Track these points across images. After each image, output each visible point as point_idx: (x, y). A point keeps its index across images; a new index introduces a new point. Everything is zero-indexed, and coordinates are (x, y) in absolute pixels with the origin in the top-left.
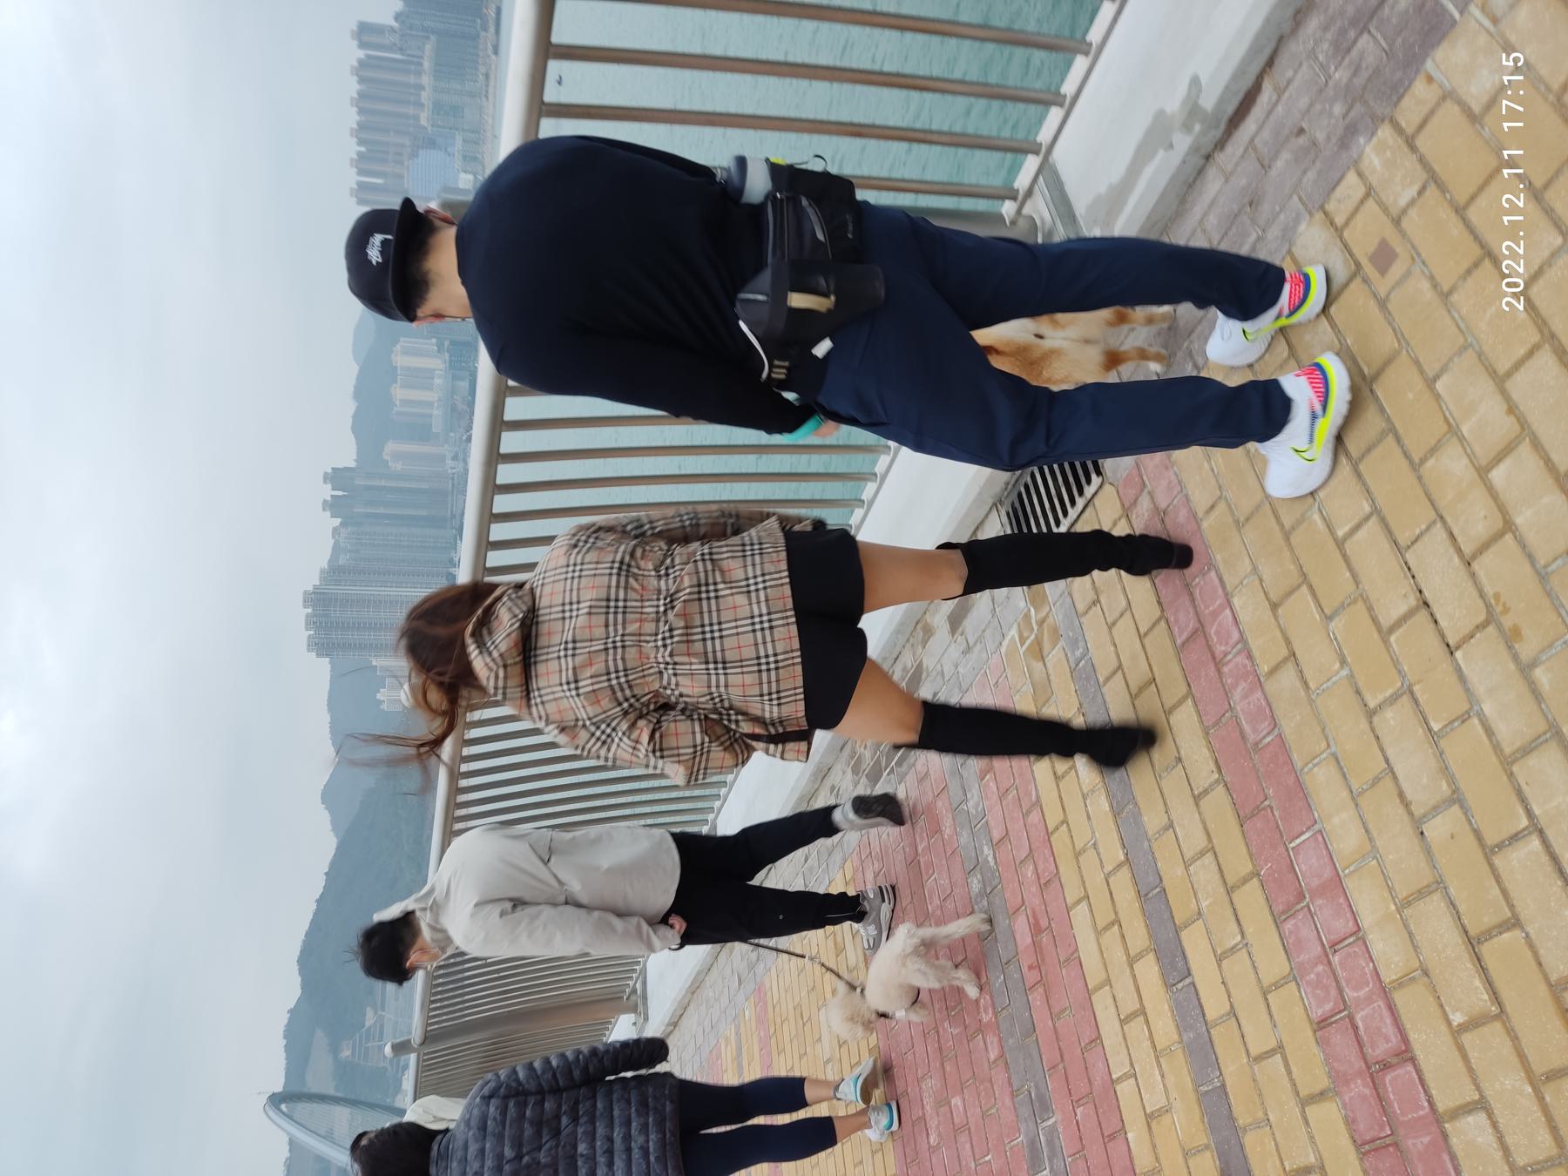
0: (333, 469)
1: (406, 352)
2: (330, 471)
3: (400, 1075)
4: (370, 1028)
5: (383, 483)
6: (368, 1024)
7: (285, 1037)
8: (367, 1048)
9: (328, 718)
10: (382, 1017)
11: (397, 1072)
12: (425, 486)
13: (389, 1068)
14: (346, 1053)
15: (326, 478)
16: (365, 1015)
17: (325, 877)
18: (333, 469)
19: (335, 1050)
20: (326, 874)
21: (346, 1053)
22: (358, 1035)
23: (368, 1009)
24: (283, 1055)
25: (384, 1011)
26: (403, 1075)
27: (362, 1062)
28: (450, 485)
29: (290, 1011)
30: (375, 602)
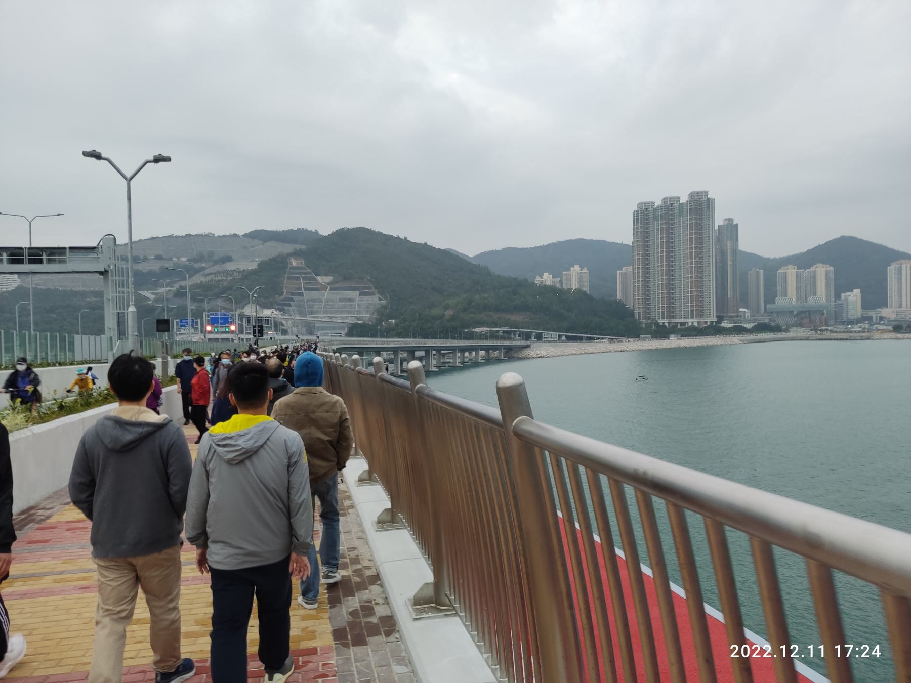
0: (737, 224)
1: (827, 273)
2: (735, 222)
3: (276, 307)
4: (316, 280)
5: (729, 263)
6: (319, 278)
7: (298, 229)
8: (298, 278)
9: (499, 248)
10: (325, 289)
11: (278, 305)
12: (730, 294)
13: (283, 297)
14: (294, 263)
15: (730, 220)
16: (326, 275)
17: (423, 243)
18: (737, 224)
19: (296, 254)
20: (426, 244)
21: (294, 263)
22: (309, 271)
23: (331, 278)
24: (286, 229)
25: (331, 290)
26: (276, 309)
27: (286, 275)
28: (733, 315)
29: (316, 232)
30: (701, 253)
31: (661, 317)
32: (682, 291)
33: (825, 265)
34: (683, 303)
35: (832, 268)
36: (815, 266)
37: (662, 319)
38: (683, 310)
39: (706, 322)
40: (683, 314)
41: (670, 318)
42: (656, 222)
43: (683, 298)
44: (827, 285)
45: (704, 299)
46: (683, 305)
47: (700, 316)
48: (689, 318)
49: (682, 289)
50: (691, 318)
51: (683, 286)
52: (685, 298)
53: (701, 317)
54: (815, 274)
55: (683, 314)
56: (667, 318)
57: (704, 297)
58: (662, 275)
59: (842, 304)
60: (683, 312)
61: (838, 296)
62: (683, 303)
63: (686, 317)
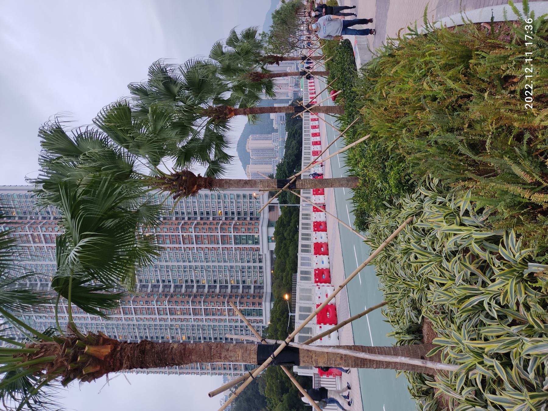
31: (258, 318)
32: (193, 264)
33: (248, 142)
34: (222, 264)
35: (250, 136)
36: (248, 151)
37: (261, 315)
38: (240, 264)
39: (271, 208)
40: (251, 264)
41: (261, 297)
42: (37, 321)
43: (210, 264)
44: (266, 139)
45: (210, 210)
46: (228, 264)
47: (253, 222)
48: (258, 250)
49: (187, 264)
50: (257, 243)
51: (181, 264)
52: (209, 256)
53: (258, 219)
54: (254, 150)
55: (251, 264)
56: (260, 304)
57: (204, 210)
58: (150, 311)
59: (281, 116)
60: (246, 264)
61: (276, 131)
62: (222, 264)
63: (257, 257)
